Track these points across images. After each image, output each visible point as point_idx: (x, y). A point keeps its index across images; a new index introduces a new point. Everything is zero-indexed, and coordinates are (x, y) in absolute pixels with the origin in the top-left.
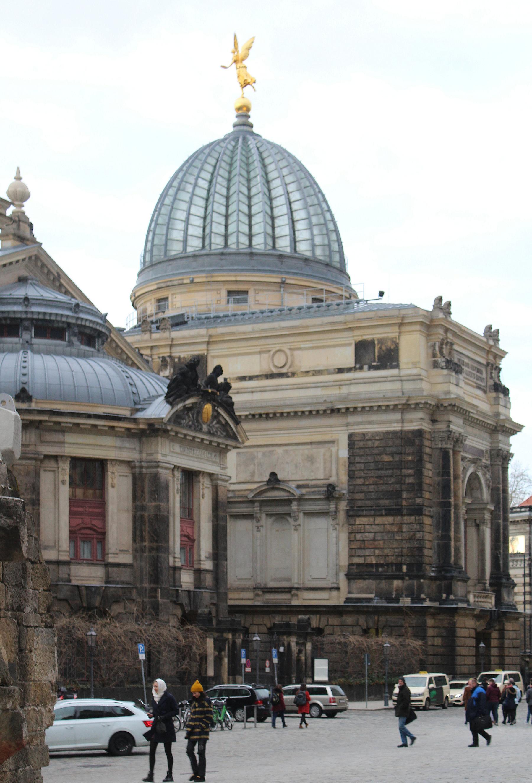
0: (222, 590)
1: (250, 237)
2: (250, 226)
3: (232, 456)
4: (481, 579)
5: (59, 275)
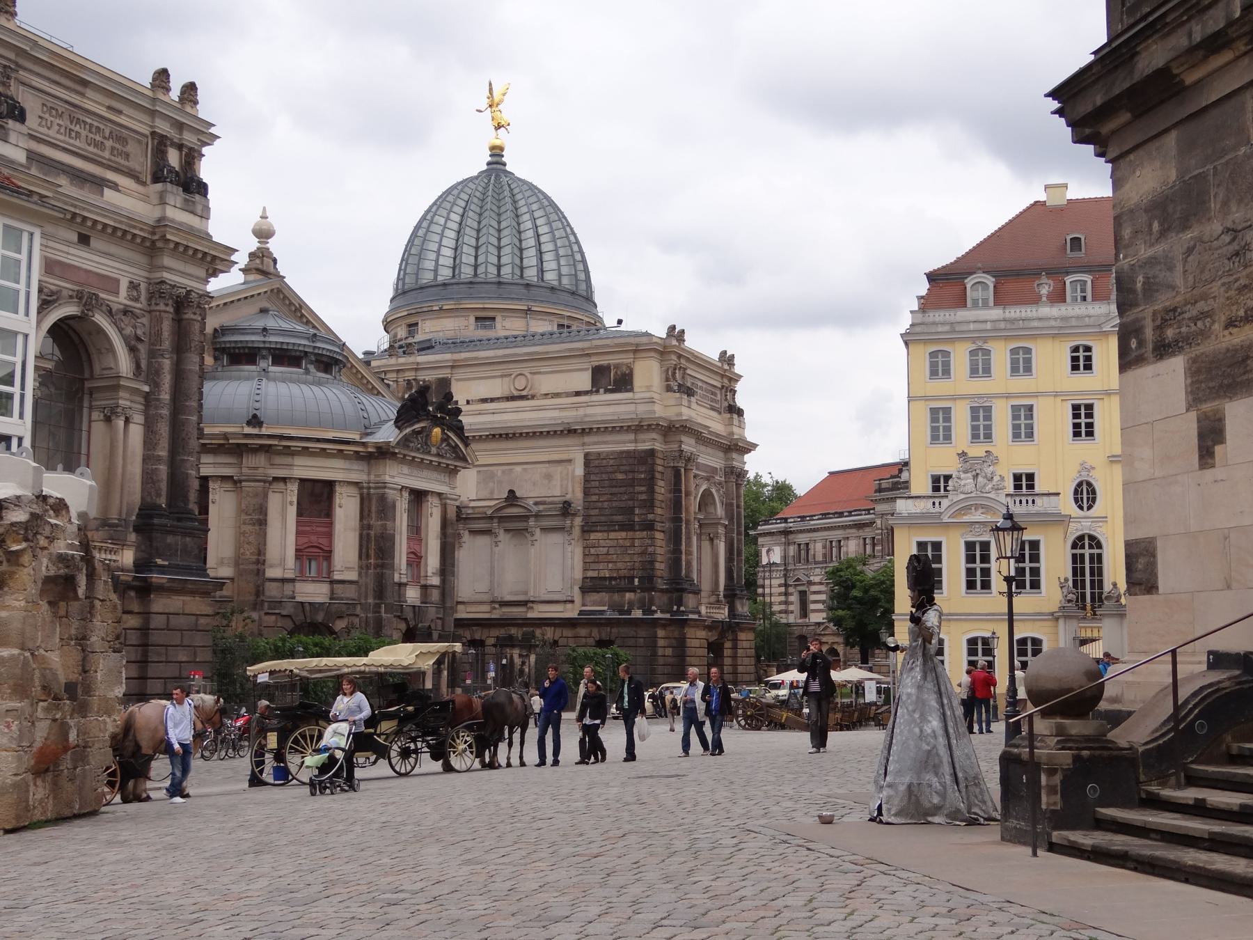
0: (448, 605)
1: (499, 267)
2: (499, 257)
3: (463, 474)
4: (715, 591)
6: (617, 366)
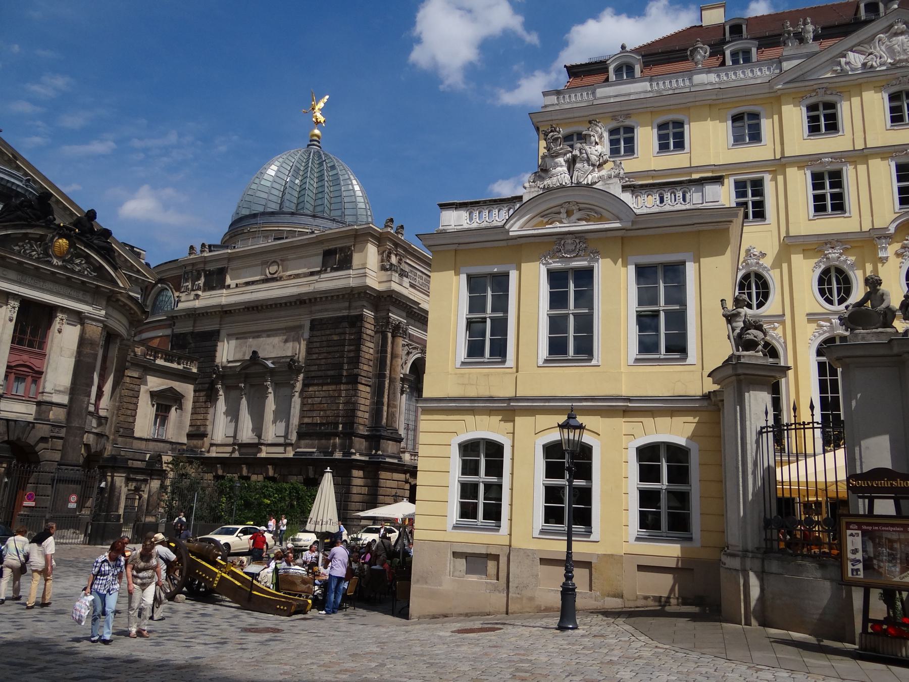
6: (342, 249)
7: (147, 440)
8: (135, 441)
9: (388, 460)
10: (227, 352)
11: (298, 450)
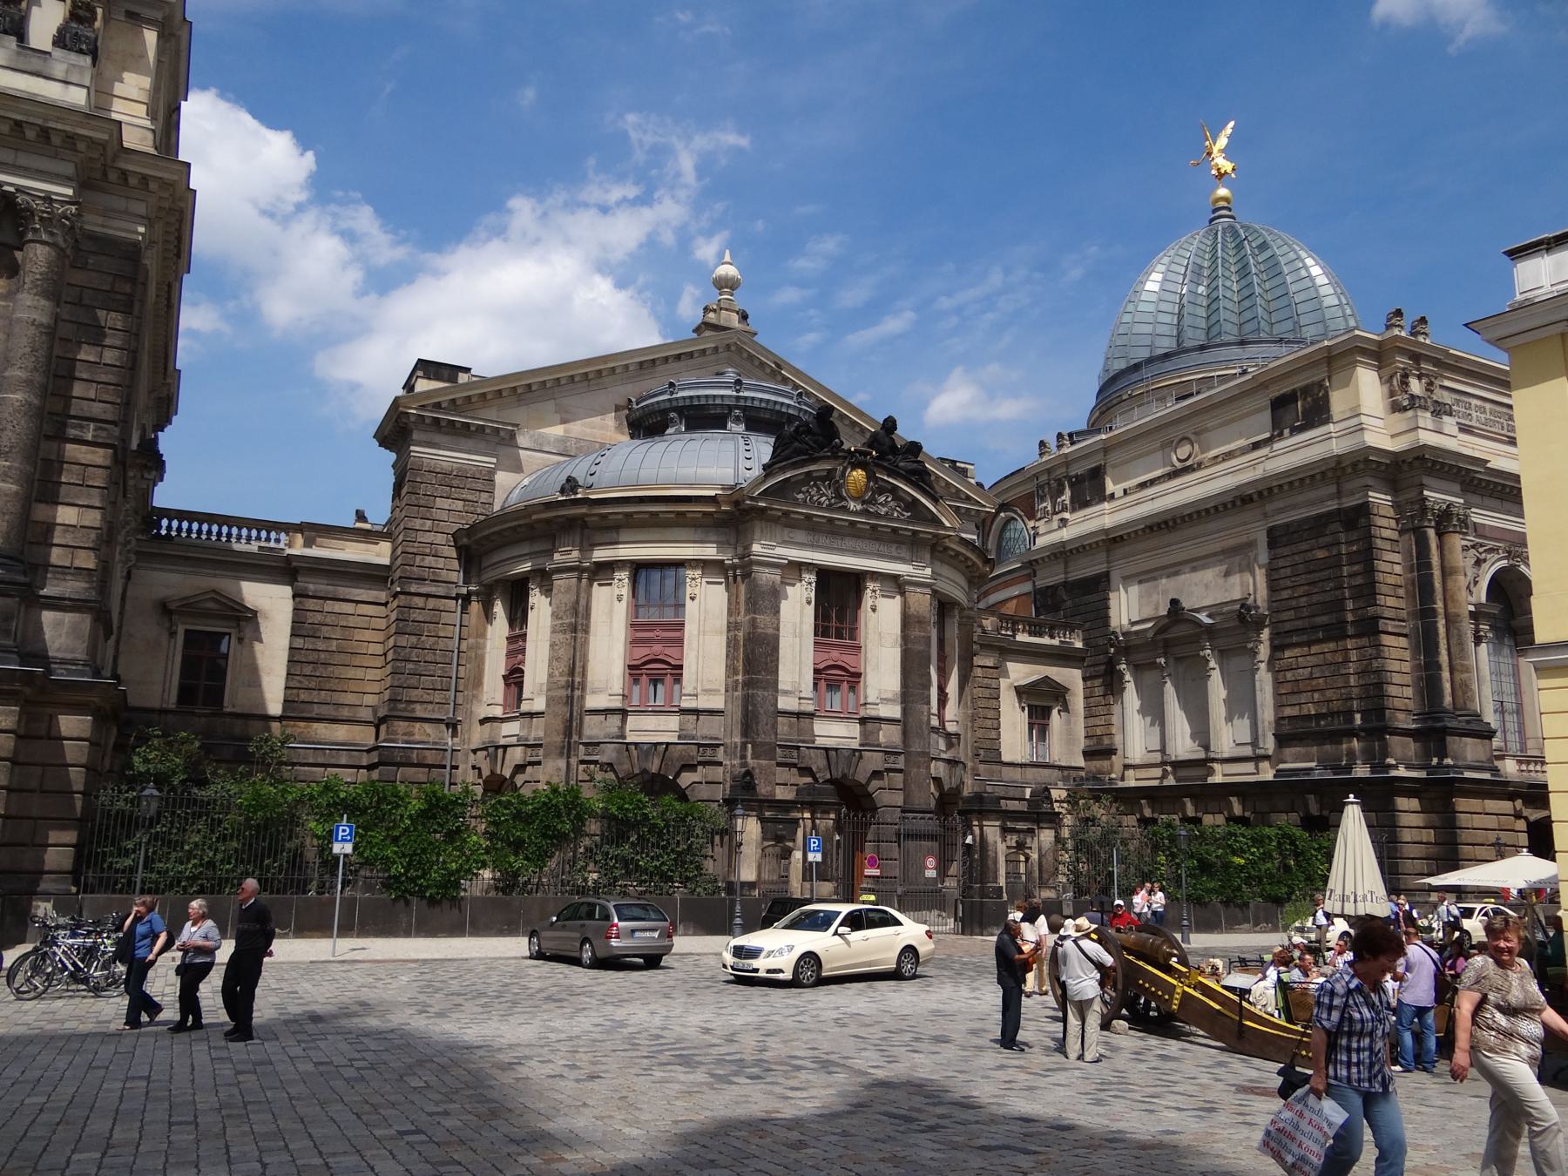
5: (778, 366)
6: (1306, 390)
7: (1022, 765)
8: (1005, 769)
9: (1468, 774)
10: (1128, 608)
11: (1282, 766)
